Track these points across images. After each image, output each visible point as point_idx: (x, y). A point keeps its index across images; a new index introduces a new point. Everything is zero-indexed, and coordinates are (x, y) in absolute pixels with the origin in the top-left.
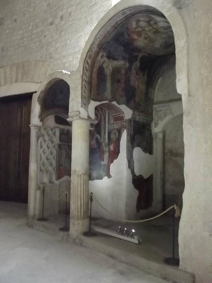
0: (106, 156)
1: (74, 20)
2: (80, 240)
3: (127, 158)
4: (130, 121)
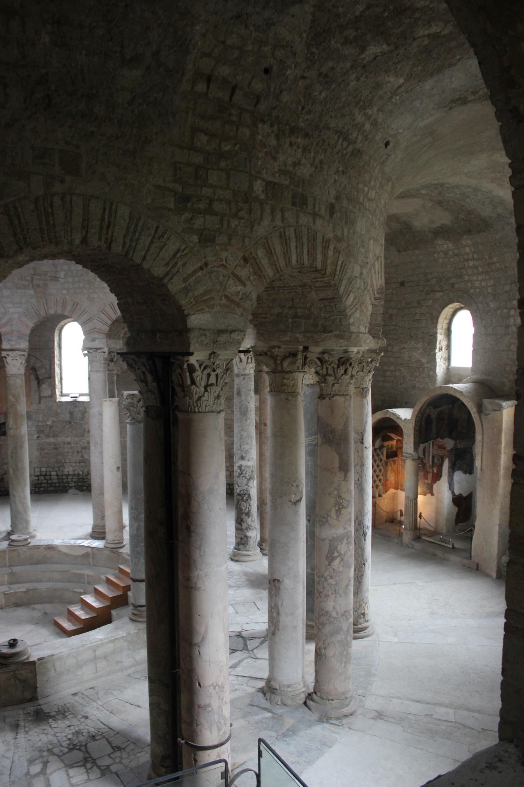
0: (430, 476)
1: (396, 325)
2: (412, 545)
3: (449, 482)
4: (452, 450)
